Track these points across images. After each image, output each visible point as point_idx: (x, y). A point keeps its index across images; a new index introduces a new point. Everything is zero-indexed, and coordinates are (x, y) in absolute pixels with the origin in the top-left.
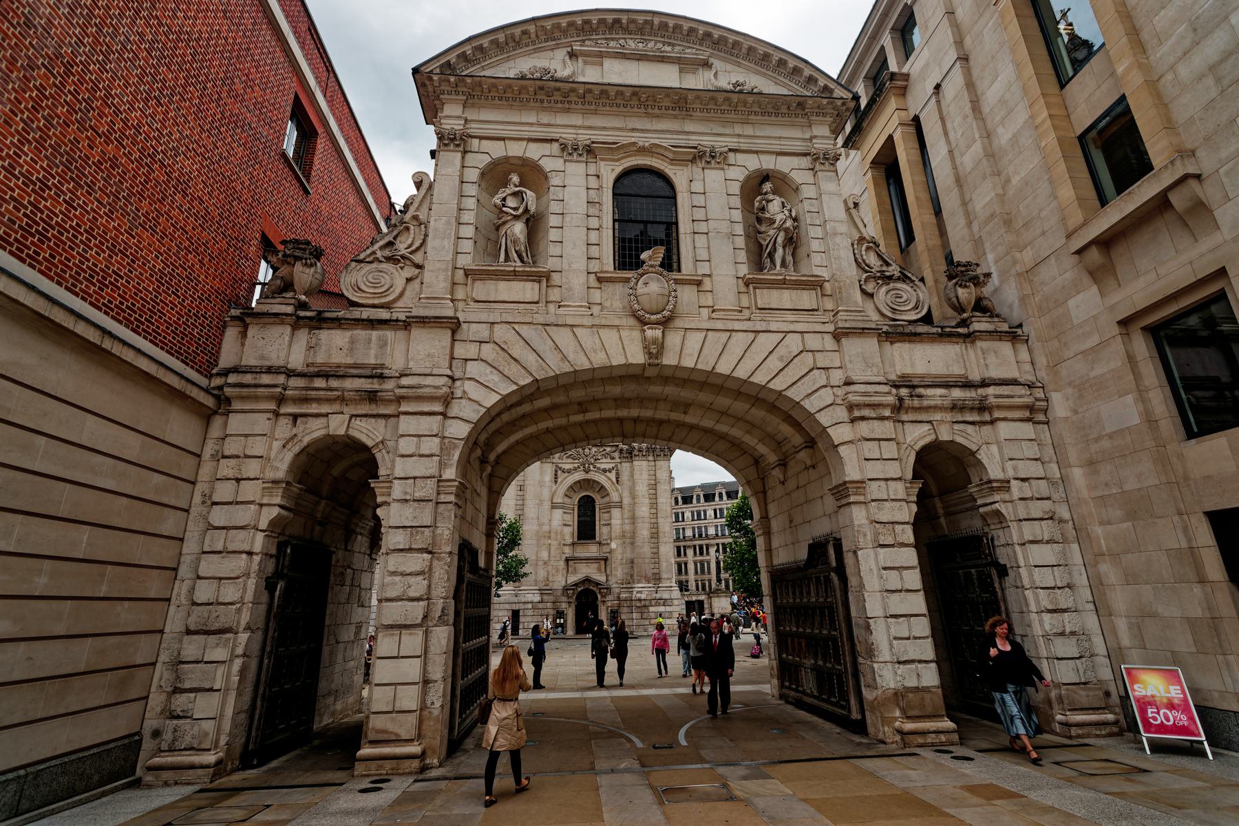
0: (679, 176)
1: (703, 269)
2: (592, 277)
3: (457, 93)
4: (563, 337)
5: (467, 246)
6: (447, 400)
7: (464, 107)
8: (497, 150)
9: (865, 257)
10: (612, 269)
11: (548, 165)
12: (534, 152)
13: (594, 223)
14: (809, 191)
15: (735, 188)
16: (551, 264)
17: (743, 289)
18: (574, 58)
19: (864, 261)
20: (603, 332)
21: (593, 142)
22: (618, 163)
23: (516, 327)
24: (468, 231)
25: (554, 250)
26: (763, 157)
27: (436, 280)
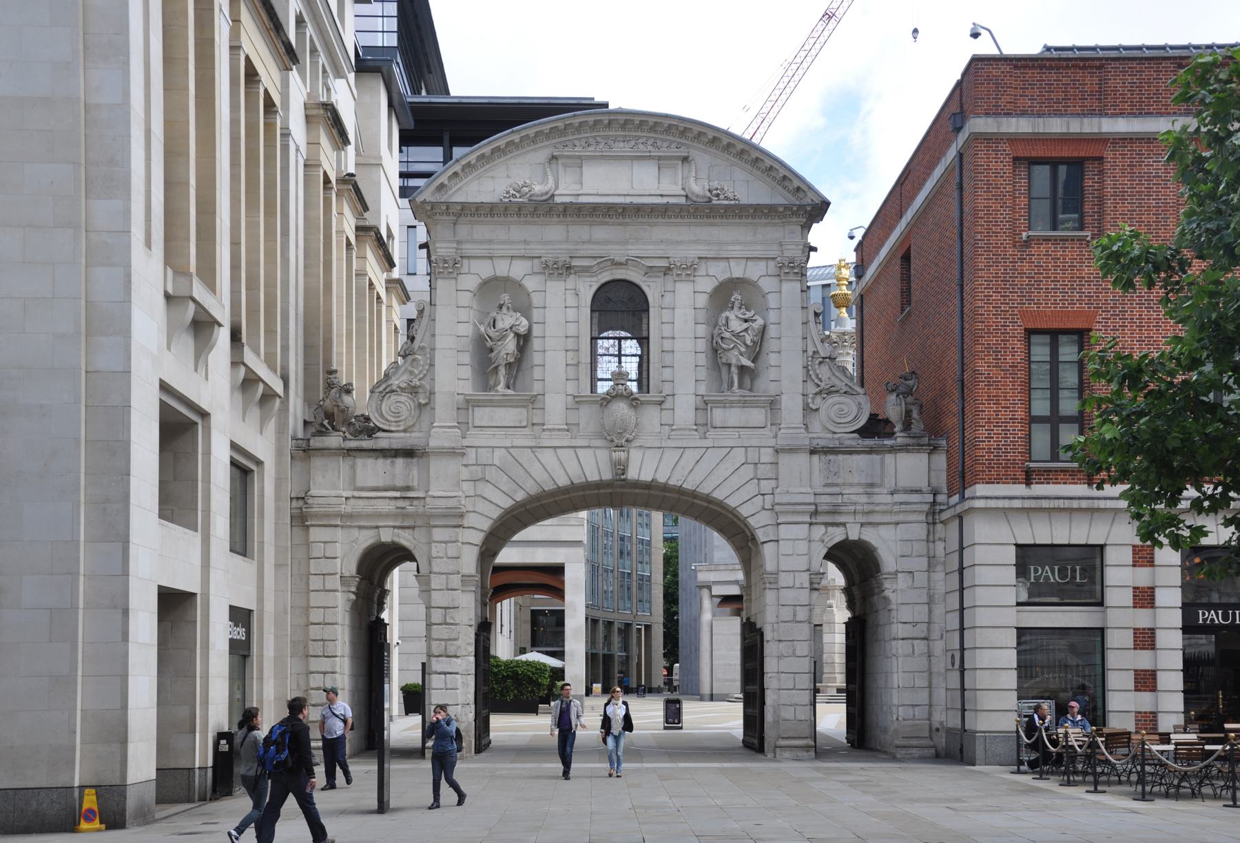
0: (652, 290)
1: (667, 389)
2: (570, 398)
3: (448, 214)
4: (547, 457)
5: (467, 372)
6: (462, 516)
7: (454, 224)
8: (485, 270)
9: (818, 371)
10: (588, 393)
11: (531, 284)
12: (518, 270)
13: (571, 344)
14: (772, 301)
15: (702, 300)
16: (537, 388)
17: (702, 405)
18: (554, 161)
19: (817, 375)
20: (581, 452)
21: (571, 257)
22: (593, 279)
23: (511, 450)
24: (466, 358)
25: (537, 373)
26: (732, 263)
27: (444, 413)
